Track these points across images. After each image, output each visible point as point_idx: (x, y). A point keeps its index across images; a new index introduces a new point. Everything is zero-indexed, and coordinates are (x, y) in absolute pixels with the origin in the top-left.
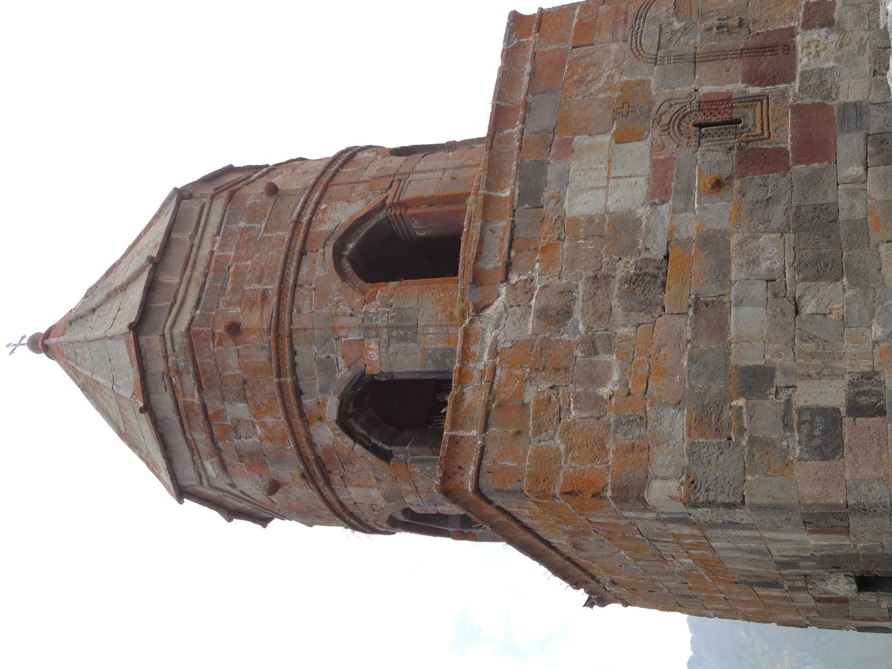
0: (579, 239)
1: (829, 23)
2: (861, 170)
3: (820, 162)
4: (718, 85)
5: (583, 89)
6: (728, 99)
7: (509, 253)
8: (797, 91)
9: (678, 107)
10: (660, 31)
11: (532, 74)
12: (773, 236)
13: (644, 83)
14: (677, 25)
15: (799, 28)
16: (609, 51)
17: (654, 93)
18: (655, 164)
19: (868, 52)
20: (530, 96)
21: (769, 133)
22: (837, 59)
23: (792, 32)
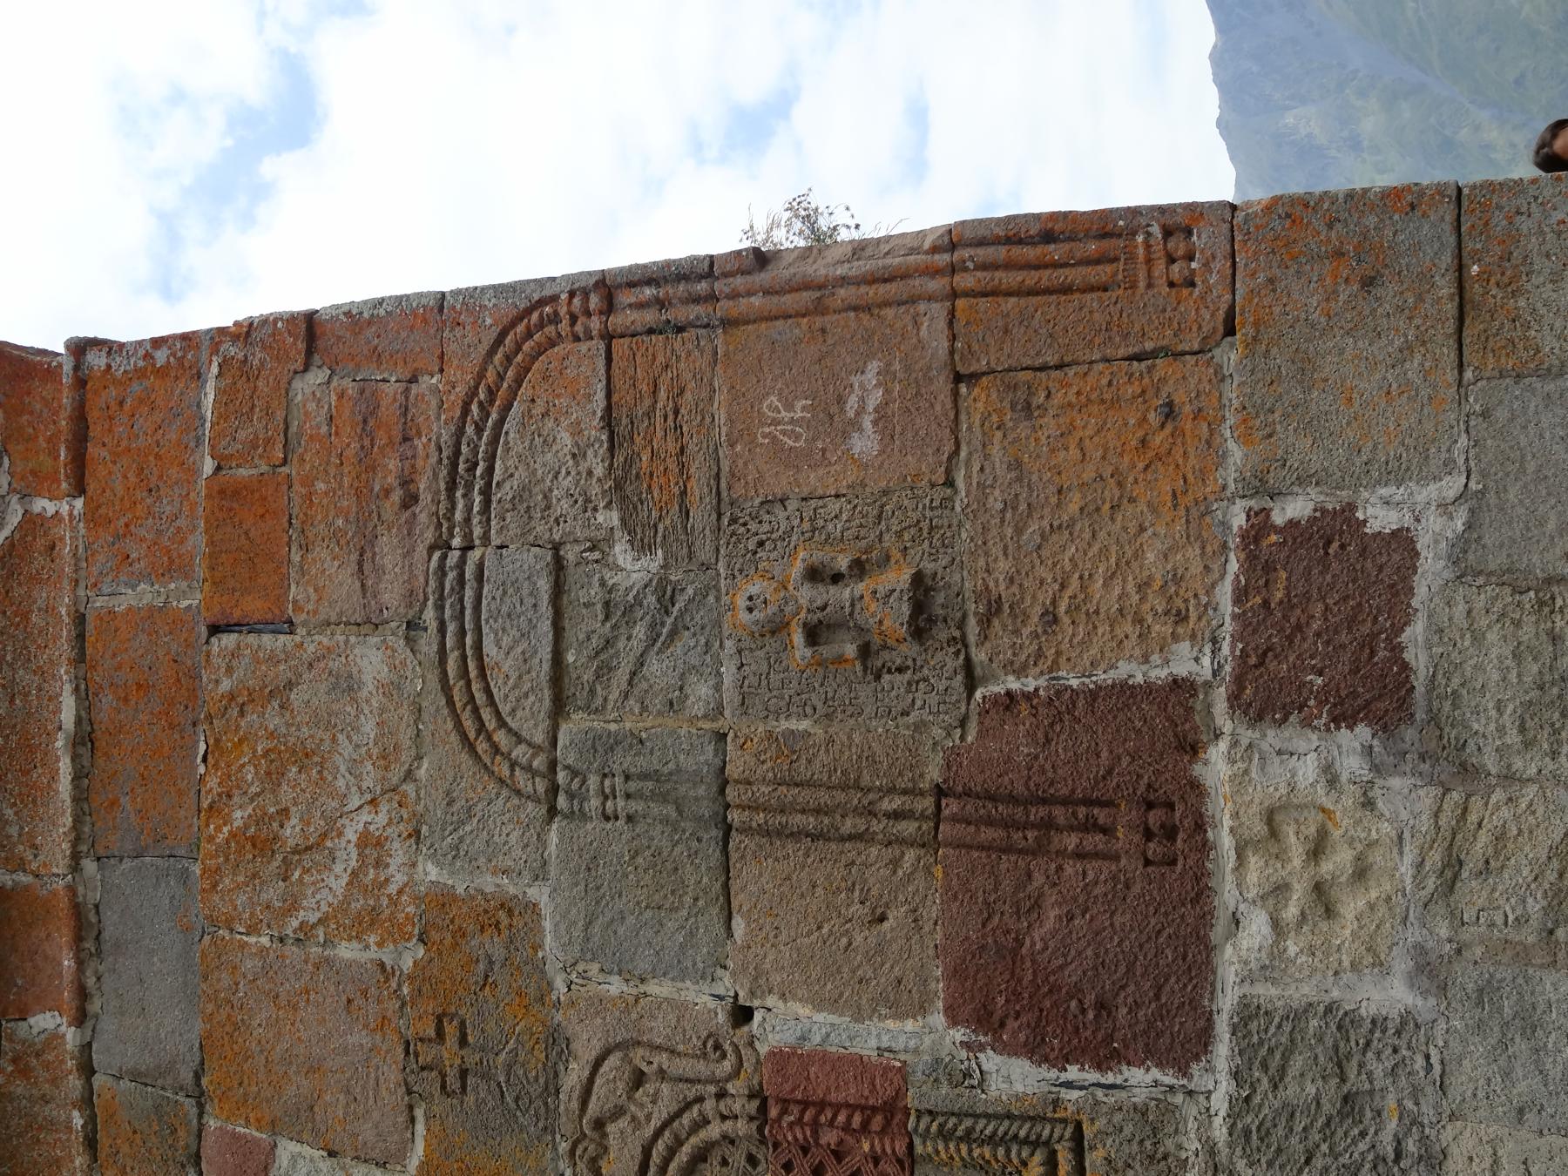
1: (1375, 694)
4: (832, 1004)
5: (273, 893)
8: (1219, 1132)
9: (668, 1097)
10: (558, 591)
11: (85, 739)
13: (506, 917)
14: (632, 568)
15: (1220, 706)
16: (347, 685)
17: (560, 984)
20: (89, 866)
22: (1429, 971)
23: (1175, 716)
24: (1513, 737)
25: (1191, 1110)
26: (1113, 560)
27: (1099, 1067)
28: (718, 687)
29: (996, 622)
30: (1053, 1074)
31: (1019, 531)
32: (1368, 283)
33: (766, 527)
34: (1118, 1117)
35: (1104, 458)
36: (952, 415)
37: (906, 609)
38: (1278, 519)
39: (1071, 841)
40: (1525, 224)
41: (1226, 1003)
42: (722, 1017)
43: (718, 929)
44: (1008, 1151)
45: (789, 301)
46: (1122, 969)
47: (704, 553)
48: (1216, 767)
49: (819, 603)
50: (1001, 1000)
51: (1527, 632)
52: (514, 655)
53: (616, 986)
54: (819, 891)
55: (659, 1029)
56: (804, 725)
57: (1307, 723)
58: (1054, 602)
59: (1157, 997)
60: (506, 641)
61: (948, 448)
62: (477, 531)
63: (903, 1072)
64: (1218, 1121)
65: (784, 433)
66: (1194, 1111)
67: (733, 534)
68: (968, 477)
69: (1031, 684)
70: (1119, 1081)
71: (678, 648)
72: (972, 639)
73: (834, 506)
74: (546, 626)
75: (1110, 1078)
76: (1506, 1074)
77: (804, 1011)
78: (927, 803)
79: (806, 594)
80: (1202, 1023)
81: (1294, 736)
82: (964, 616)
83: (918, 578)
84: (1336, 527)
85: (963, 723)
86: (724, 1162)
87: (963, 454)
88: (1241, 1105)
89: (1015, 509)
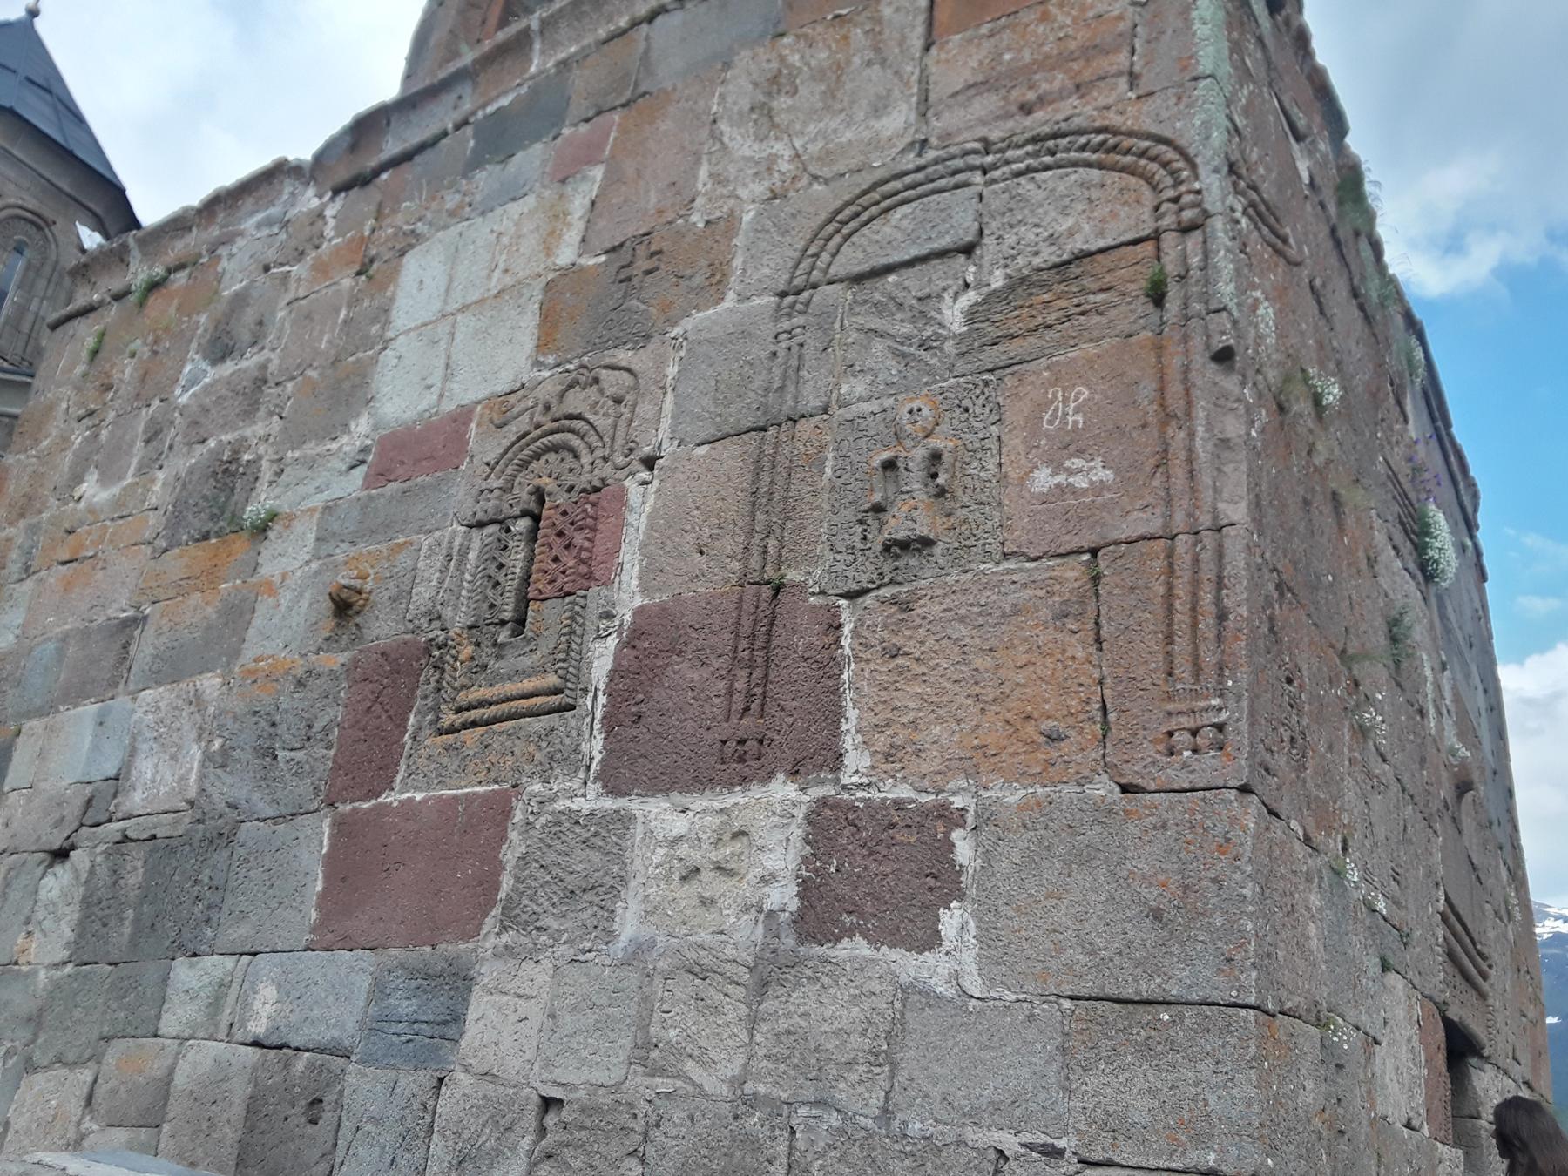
0: (349, 307)
1: (820, 914)
2: (257, 1027)
3: (323, 896)
6: (589, 576)
7: (383, 167)
8: (560, 805)
12: (193, 777)
15: (818, 792)
16: (879, 108)
18: (462, 416)
19: (641, 1085)
21: (452, 730)
22: (639, 951)
24: (783, 1025)
25: (576, 784)
26: (935, 699)
27: (604, 718)
28: (861, 399)
29: (895, 608)
30: (602, 686)
31: (962, 619)
32: (1157, 914)
33: (978, 411)
34: (574, 733)
35: (1018, 684)
36: (1060, 551)
37: (901, 535)
38: (956, 835)
39: (740, 685)
40: (1207, 1067)
41: (634, 805)
42: (647, 450)
43: (703, 436)
44: (564, 661)
45: (1175, 388)
46: (659, 729)
47: (961, 367)
48: (782, 790)
49: (911, 465)
50: (646, 645)
51: (856, 1041)
52: (894, 234)
53: (672, 370)
54: (720, 503)
55: (645, 409)
56: (828, 471)
57: (805, 860)
58: (906, 654)
59: (641, 756)
60: (905, 223)
61: (1033, 553)
62: (996, 174)
63: (607, 583)
64: (568, 803)
65: (1056, 410)
66: (575, 786)
67: (976, 386)
68: (1008, 572)
69: (845, 642)
70: (595, 732)
71: (891, 363)
72: (884, 592)
73: (991, 465)
74: (915, 252)
75: (597, 726)
76: (574, 1009)
77: (648, 508)
78: (770, 573)
79: (919, 453)
80: (624, 788)
81: (797, 849)
82: (900, 583)
83: (927, 542)
84: (944, 881)
85: (822, 593)
86: (571, 470)
87: (1028, 565)
88: (573, 817)
89: (980, 614)
